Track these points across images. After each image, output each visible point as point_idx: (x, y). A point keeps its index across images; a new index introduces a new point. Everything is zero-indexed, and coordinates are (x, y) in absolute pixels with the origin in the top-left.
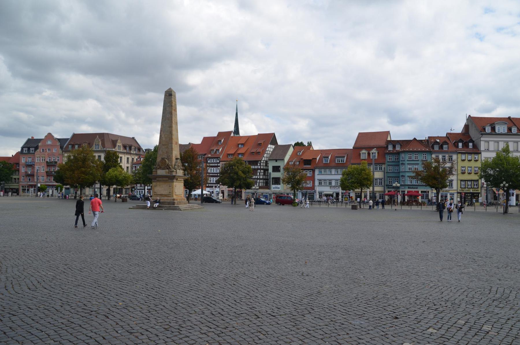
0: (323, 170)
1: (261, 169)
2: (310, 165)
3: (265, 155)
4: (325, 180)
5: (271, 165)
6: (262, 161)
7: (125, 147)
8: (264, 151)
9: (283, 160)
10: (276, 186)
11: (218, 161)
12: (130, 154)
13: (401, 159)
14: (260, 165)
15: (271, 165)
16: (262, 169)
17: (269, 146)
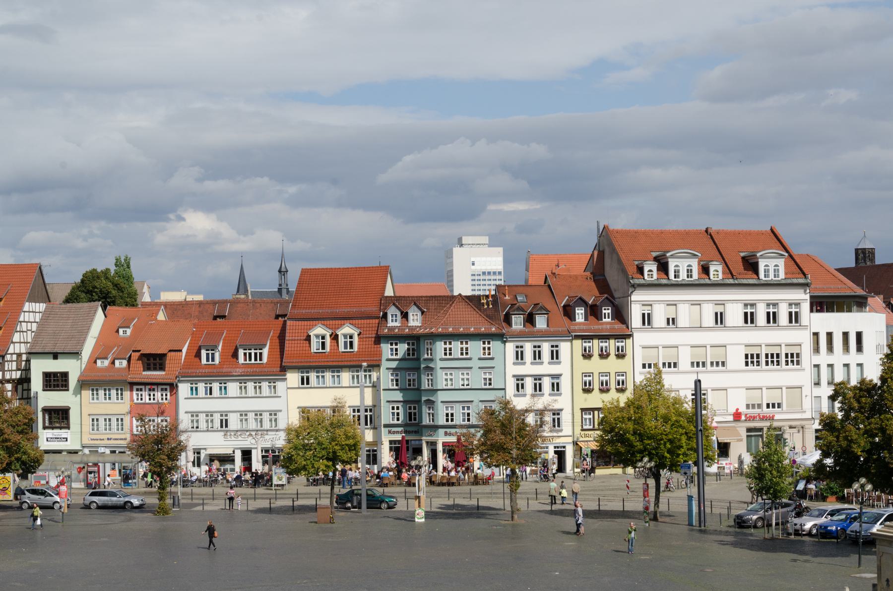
0: (201, 386)
2: (162, 368)
3: (16, 337)
4: (209, 414)
5: (39, 367)
6: (8, 357)
10: (57, 432)
15: (39, 367)
16: (8, 381)
17: (27, 306)
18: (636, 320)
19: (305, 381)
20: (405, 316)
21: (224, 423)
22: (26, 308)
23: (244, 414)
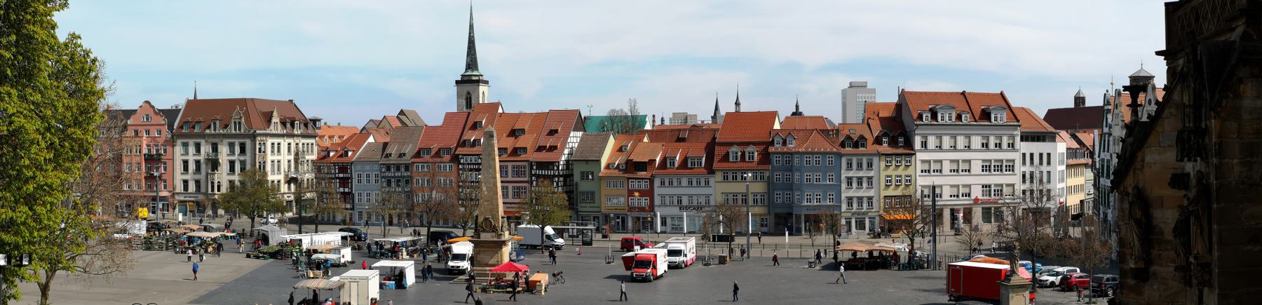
1: (559, 176)
3: (566, 151)
4: (671, 196)
7: (284, 124)
8: (565, 143)
9: (599, 161)
12: (292, 136)
18: (917, 145)
19: (725, 178)
20: (784, 143)
21: (680, 202)
23: (690, 196)
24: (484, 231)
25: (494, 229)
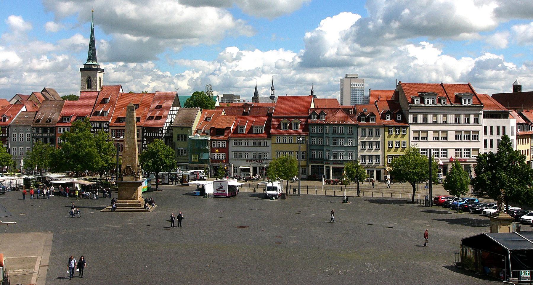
3: (167, 121)
4: (241, 153)
9: (191, 128)
11: (106, 126)
13: (325, 132)
14: (162, 133)
18: (411, 120)
19: (278, 141)
21: (247, 156)
22: (171, 109)
24: (126, 175)
25: (133, 174)
